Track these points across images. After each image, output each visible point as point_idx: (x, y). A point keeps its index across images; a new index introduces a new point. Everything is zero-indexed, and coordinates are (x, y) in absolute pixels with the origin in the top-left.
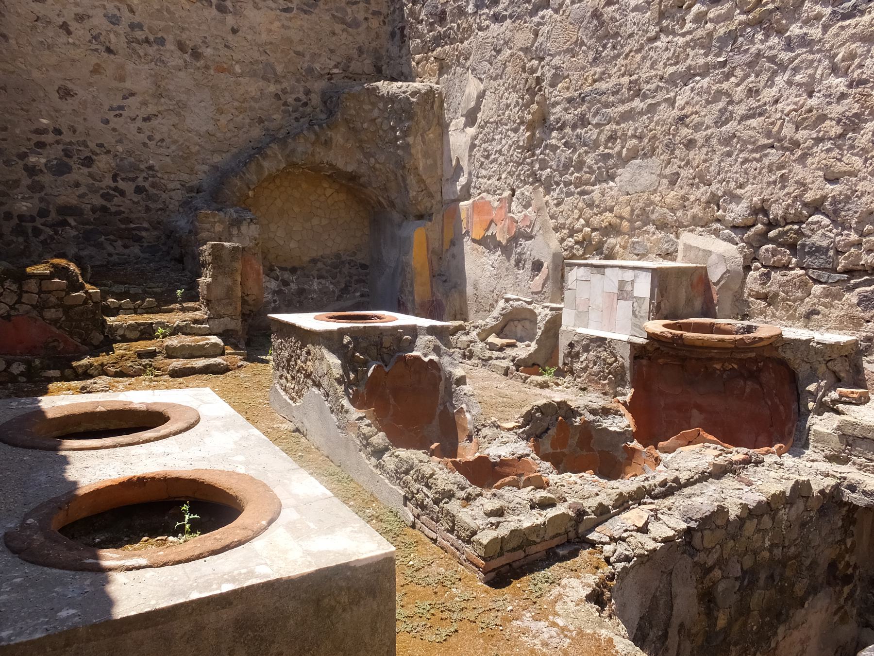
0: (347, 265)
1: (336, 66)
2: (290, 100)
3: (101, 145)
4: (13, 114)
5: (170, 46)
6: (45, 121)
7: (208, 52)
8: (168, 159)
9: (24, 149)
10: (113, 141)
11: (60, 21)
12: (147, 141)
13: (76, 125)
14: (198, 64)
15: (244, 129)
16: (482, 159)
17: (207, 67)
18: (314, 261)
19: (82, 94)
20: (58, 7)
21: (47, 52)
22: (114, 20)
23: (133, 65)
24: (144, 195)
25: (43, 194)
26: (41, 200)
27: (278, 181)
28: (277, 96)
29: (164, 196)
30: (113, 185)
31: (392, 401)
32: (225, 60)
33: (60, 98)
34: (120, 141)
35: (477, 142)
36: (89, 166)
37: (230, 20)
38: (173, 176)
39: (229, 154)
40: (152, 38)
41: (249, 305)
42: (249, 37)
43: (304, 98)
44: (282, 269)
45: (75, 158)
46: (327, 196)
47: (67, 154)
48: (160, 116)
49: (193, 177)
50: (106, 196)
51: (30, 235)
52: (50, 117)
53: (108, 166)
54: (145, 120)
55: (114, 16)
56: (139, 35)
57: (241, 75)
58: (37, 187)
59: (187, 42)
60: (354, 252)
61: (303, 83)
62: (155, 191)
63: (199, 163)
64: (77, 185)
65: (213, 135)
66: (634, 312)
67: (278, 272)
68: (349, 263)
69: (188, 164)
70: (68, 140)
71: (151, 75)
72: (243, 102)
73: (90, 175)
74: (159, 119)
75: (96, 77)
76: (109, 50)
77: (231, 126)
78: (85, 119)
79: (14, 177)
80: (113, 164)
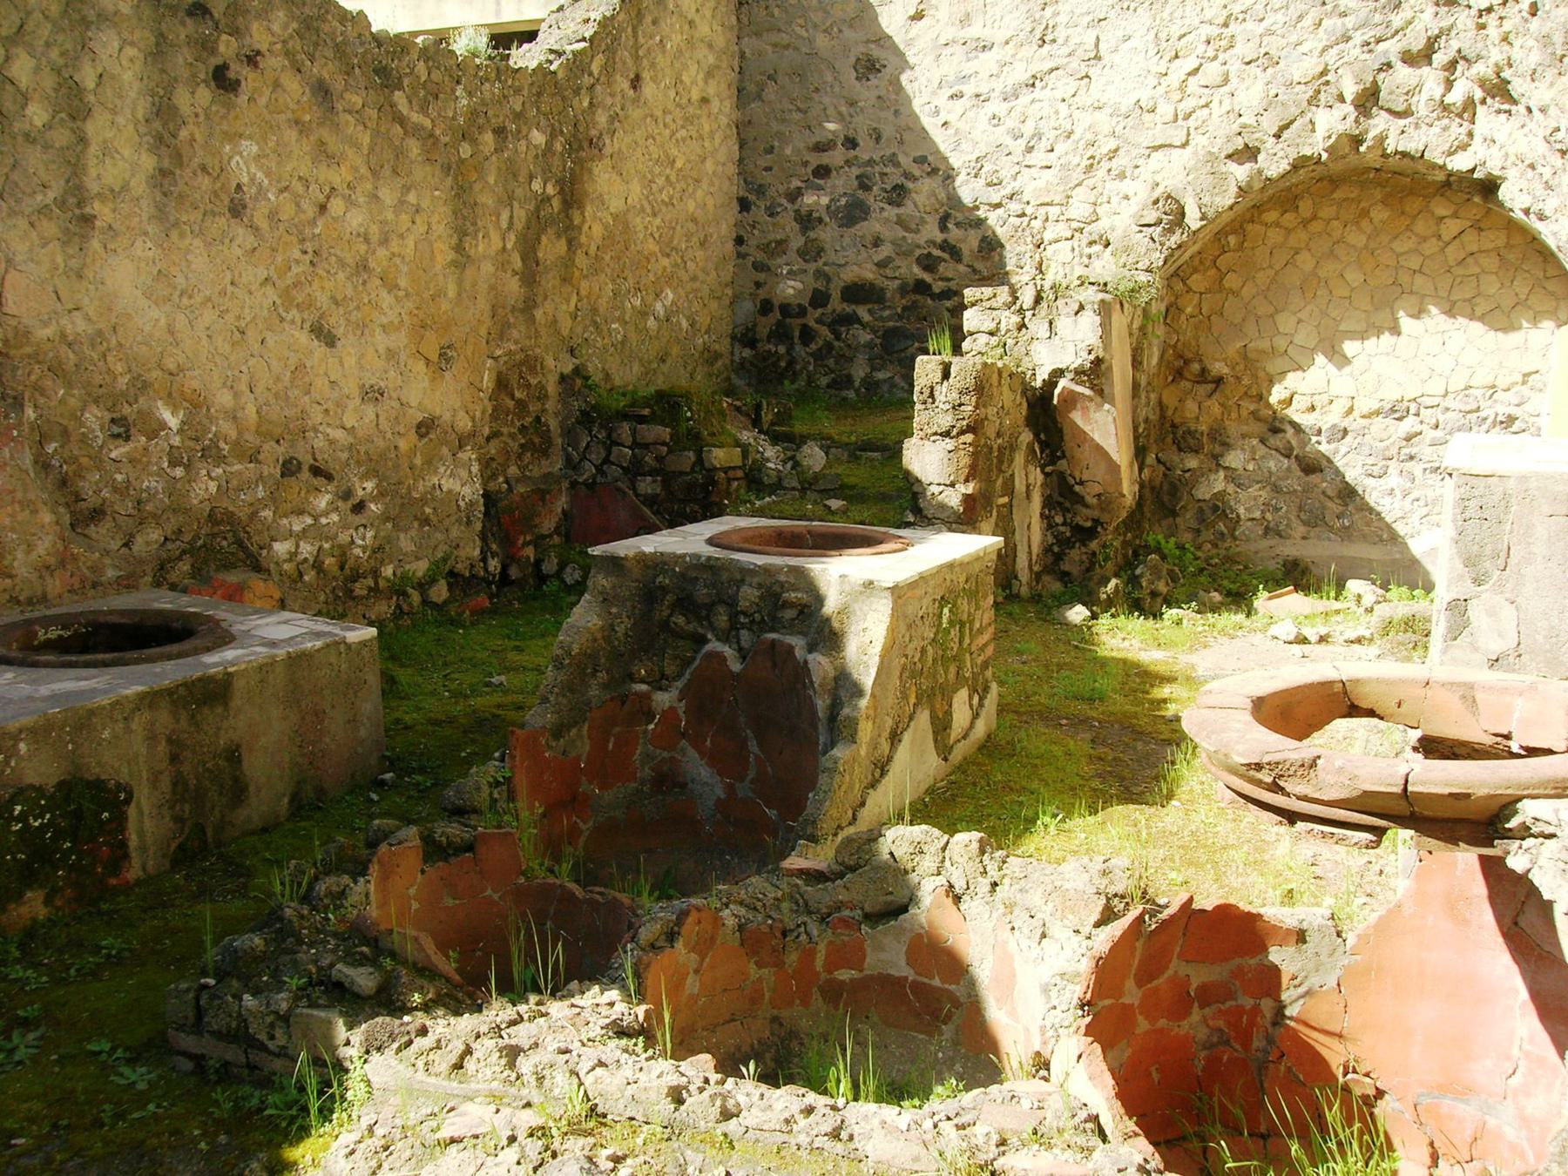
3: (921, 160)
6: (831, 126)
9: (796, 183)
13: (881, 127)
26: (819, 274)
27: (1305, 207)
31: (753, 746)
36: (899, 205)
39: (1189, 149)
41: (1087, 506)
46: (1446, 238)
47: (864, 184)
50: (928, 263)
52: (841, 118)
53: (933, 200)
58: (811, 252)
64: (877, 242)
70: (866, 157)
73: (900, 222)
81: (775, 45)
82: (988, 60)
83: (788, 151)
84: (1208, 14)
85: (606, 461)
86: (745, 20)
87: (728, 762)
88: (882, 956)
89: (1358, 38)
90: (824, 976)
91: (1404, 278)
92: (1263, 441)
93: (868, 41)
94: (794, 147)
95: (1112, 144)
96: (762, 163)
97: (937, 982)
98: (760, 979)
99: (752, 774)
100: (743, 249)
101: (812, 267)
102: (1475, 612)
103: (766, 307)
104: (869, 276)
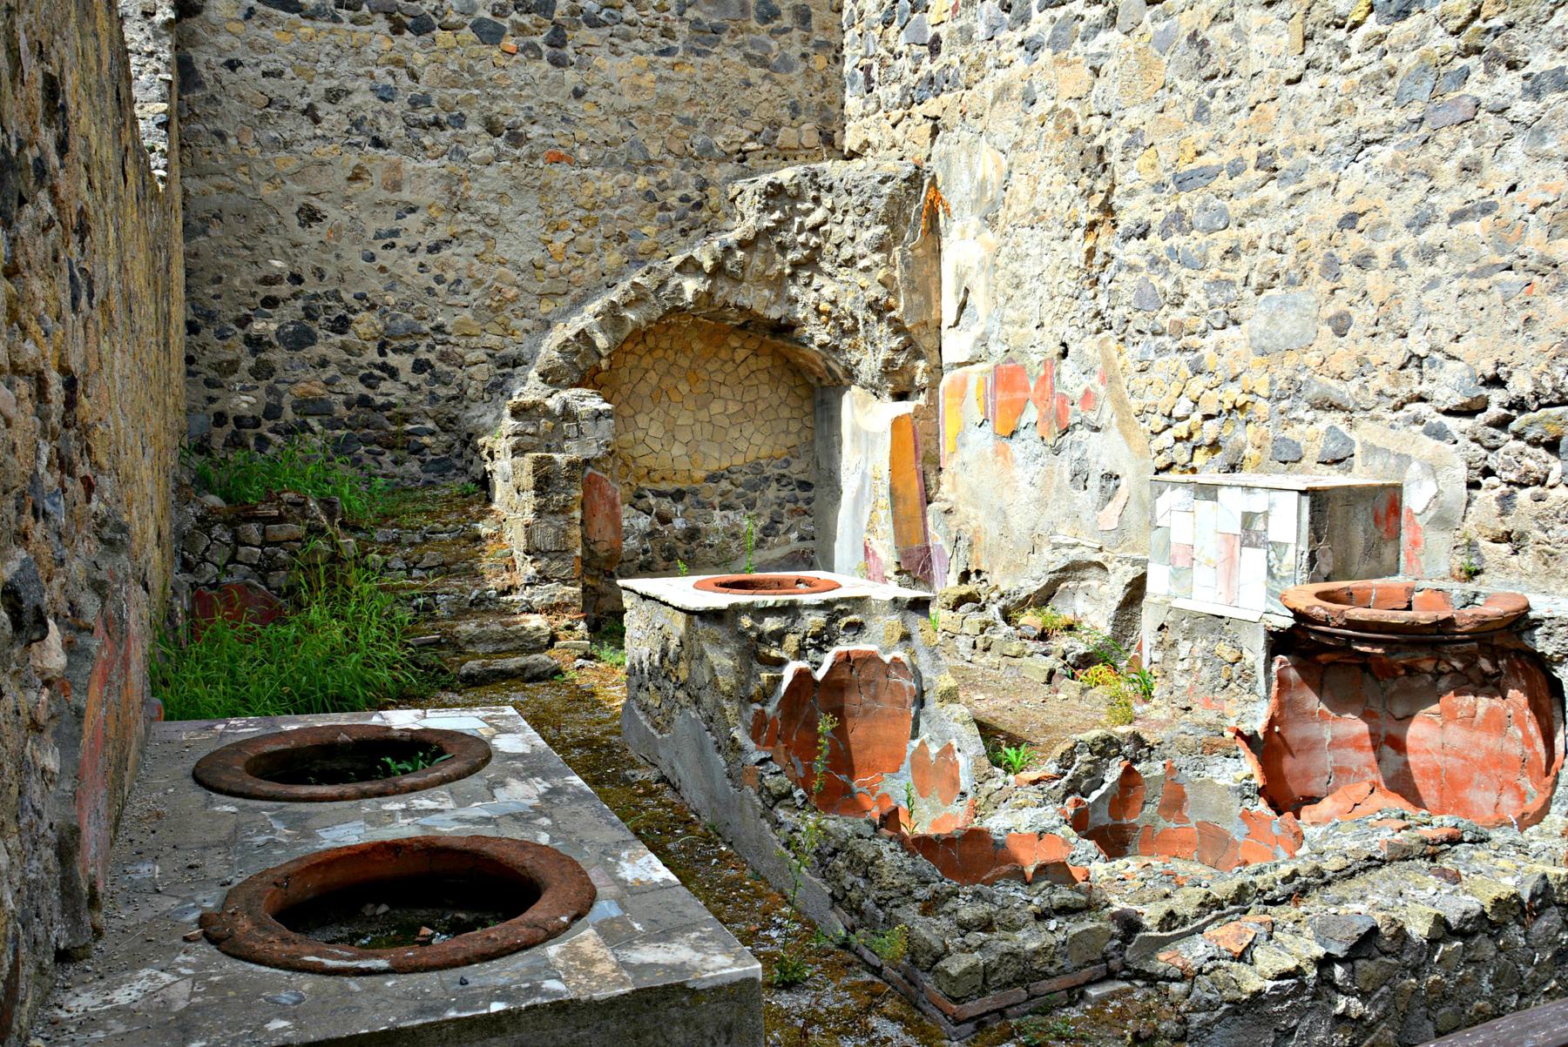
0: (774, 485)
1: (752, 139)
2: (673, 200)
3: (361, 297)
4: (231, 255)
5: (473, 128)
6: (277, 263)
7: (535, 131)
8: (467, 313)
9: (245, 311)
10: (380, 288)
12: (433, 284)
13: (324, 266)
14: (518, 153)
15: (594, 255)
16: (1010, 291)
17: (533, 157)
18: (714, 478)
19: (333, 214)
20: (300, 82)
21: (283, 154)
22: (386, 95)
23: (414, 163)
24: (426, 375)
25: (272, 380)
26: (271, 391)
27: (650, 341)
28: (649, 196)
29: (460, 374)
30: (379, 360)
32: (562, 141)
33: (301, 225)
34: (390, 288)
35: (1001, 261)
36: (342, 333)
37: (571, 76)
38: (474, 339)
40: (444, 117)
42: (602, 102)
43: (696, 196)
44: (659, 494)
45: (321, 321)
47: (310, 314)
49: (508, 340)
51: (253, 448)
52: (285, 256)
54: (430, 250)
55: (386, 87)
56: (426, 114)
57: (588, 165)
58: (263, 371)
59: (502, 119)
60: (786, 461)
61: (693, 170)
64: (324, 363)
65: (542, 268)
66: (1270, 569)
67: (653, 501)
68: (778, 481)
69: (499, 319)
70: (311, 292)
71: (442, 176)
72: (592, 209)
73: (344, 347)
74: (455, 249)
75: (357, 185)
77: (571, 252)
78: (338, 256)
79: (230, 356)
81: (219, 188)
84: (582, 200)
85: (233, 559)
86: (188, 161)
91: (715, 388)
92: (633, 506)
94: (243, 279)
100: (193, 368)
103: (220, 419)
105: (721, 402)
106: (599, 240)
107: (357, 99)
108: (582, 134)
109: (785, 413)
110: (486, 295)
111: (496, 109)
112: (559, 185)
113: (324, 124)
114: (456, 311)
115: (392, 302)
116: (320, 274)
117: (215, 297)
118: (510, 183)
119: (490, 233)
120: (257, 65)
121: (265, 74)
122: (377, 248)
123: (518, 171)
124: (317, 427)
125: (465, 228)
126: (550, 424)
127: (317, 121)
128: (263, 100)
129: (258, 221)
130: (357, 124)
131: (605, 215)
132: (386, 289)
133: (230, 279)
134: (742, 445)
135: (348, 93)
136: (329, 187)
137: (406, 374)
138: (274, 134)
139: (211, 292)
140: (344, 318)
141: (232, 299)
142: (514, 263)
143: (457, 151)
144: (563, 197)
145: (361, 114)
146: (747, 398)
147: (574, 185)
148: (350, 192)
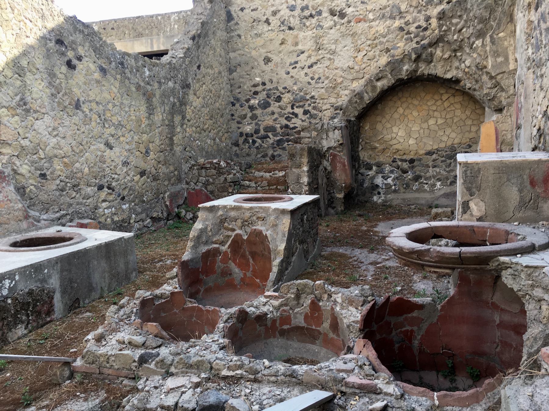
2: (412, 29)
3: (285, 88)
4: (243, 78)
5: (325, 14)
7: (349, 11)
8: (323, 90)
9: (248, 97)
10: (291, 84)
11: (264, 18)
12: (310, 81)
13: (272, 78)
14: (343, 21)
15: (375, 60)
17: (349, 22)
18: (430, 153)
19: (276, 59)
20: (263, 11)
21: (259, 38)
22: (292, 8)
23: (303, 33)
24: (308, 116)
25: (257, 120)
26: (257, 124)
28: (401, 29)
29: (320, 114)
30: (291, 111)
31: (251, 261)
32: (361, 12)
33: (265, 64)
34: (295, 84)
36: (279, 102)
39: (363, 80)
40: (314, 13)
43: (424, 25)
44: (402, 160)
45: (272, 98)
46: (444, 100)
47: (268, 96)
48: (319, 63)
49: (338, 100)
52: (260, 76)
54: (309, 67)
56: (307, 13)
57: (373, 20)
58: (254, 117)
59: (336, 8)
62: (315, 112)
63: (342, 90)
64: (273, 113)
65: (353, 68)
67: (400, 163)
69: (336, 92)
71: (313, 37)
72: (374, 40)
73: (280, 107)
74: (319, 65)
75: (283, 46)
76: (290, 28)
78: (277, 74)
79: (244, 113)
80: (292, 99)
81: (239, 55)
82: (303, 57)
83: (245, 87)
84: (369, 37)
87: (244, 266)
88: (297, 320)
89: (415, 40)
90: (279, 328)
91: (431, 113)
93: (267, 52)
94: (247, 86)
95: (342, 79)
96: (238, 91)
97: (314, 327)
98: (260, 331)
99: (251, 269)
100: (234, 117)
101: (254, 122)
102: (472, 205)
103: (241, 134)
104: (271, 124)
105: (435, 119)
106: (377, 53)
107: (282, 13)
108: (369, 7)
109: (469, 122)
110: (330, 82)
111: (333, 4)
112: (360, 32)
113: (272, 25)
114: (319, 90)
115: (296, 89)
116: (271, 81)
117: (239, 93)
118: (340, 35)
119: (332, 57)
120: (250, 7)
121: (252, 10)
122: (290, 69)
123: (343, 29)
124: (271, 136)
125: (322, 56)
126: (316, 133)
127: (269, 24)
128: (252, 20)
129: (251, 65)
130: (283, 23)
131: (380, 42)
132: (294, 84)
133: (243, 86)
134: (445, 138)
135: (279, 11)
136: (274, 49)
137: (301, 116)
138: (255, 32)
139: (238, 92)
140: (279, 96)
141: (244, 93)
142: (342, 68)
143: (319, 26)
144: (363, 37)
145: (284, 18)
146: (448, 117)
147: (367, 31)
148: (280, 49)
